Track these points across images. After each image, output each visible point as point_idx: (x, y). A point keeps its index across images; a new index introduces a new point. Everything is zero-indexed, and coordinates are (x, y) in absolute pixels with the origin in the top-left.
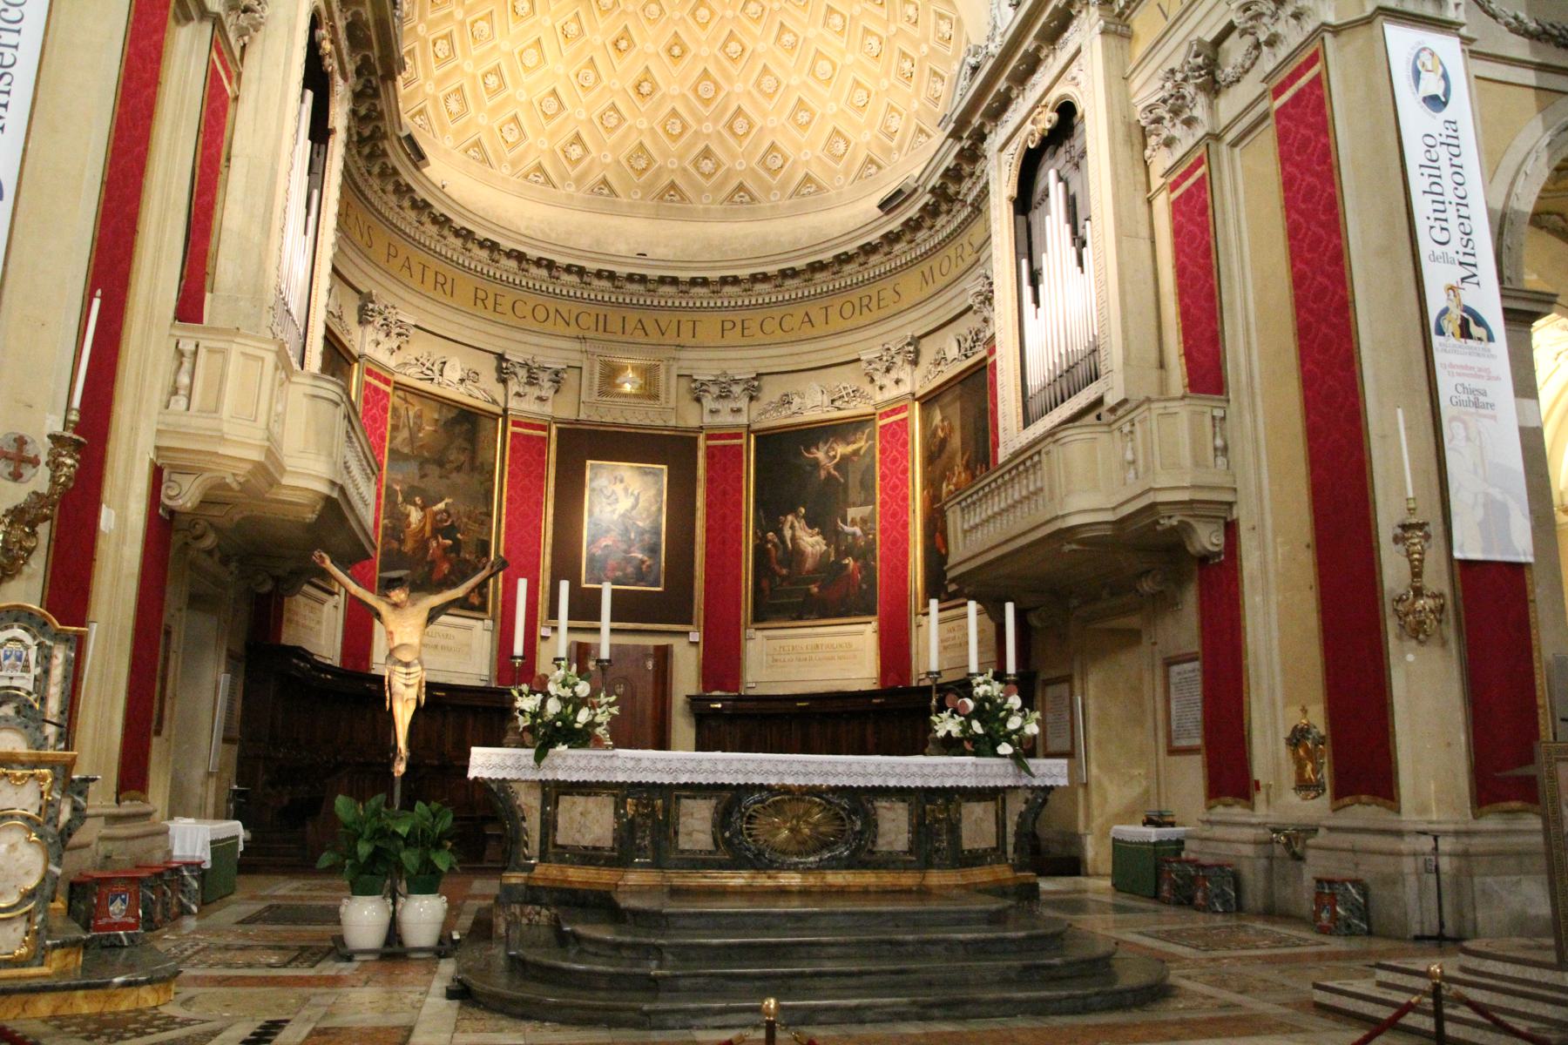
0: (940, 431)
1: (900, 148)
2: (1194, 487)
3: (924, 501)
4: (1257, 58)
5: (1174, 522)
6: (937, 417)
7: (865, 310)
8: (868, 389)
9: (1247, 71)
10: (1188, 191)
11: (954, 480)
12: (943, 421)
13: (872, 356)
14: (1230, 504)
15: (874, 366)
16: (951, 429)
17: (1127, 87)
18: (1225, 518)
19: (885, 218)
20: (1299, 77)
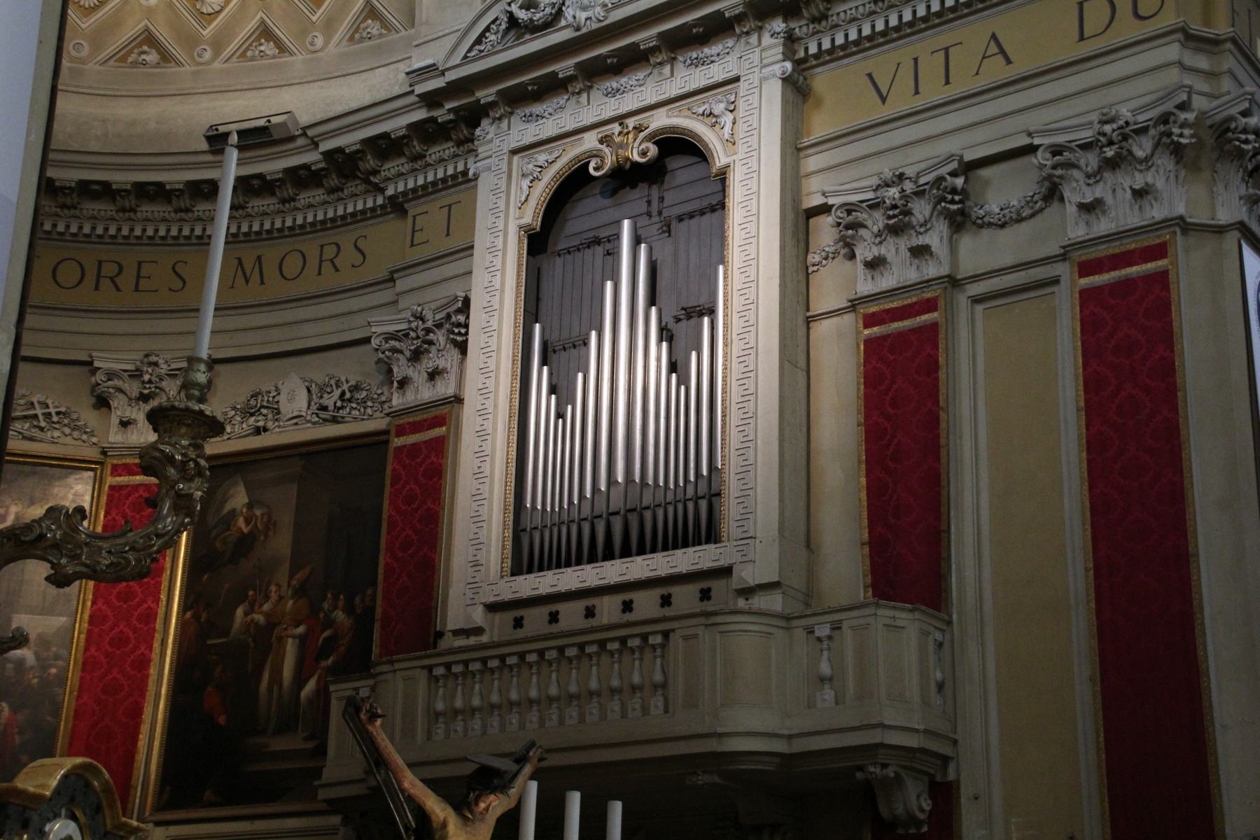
0: (241, 522)
1: (217, 45)
2: (927, 732)
3: (183, 625)
4: (1041, 210)
5: (890, 772)
6: (239, 498)
7: (106, 284)
8: (89, 417)
9: (1020, 220)
10: (901, 336)
11: (266, 607)
12: (250, 506)
13: (118, 366)
14: (945, 760)
15: (116, 382)
16: (271, 524)
17: (798, 160)
18: (931, 776)
19: (209, 158)
20: (1130, 265)
